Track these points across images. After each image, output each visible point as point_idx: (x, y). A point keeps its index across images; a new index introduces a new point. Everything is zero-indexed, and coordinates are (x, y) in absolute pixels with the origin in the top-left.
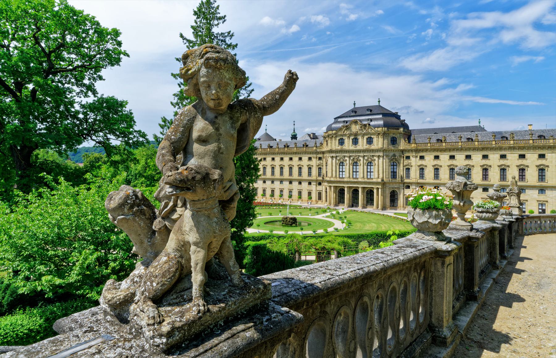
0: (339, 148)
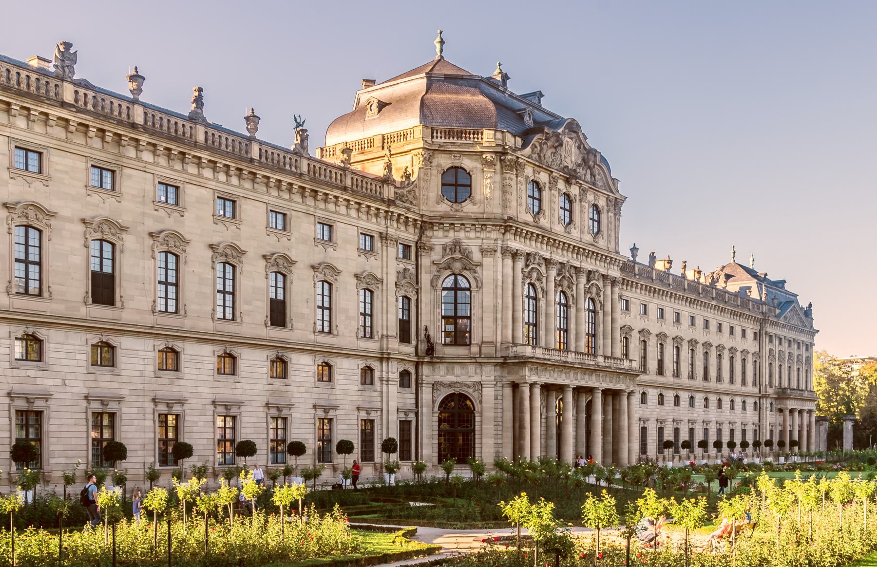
0: (529, 218)
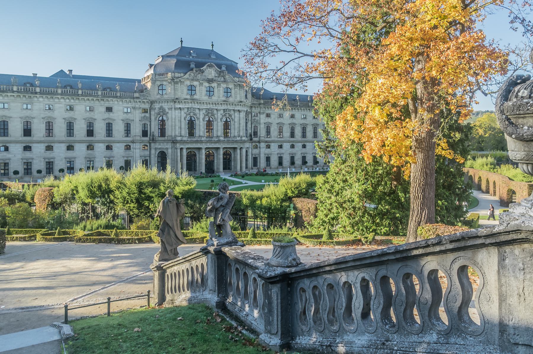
0: (188, 97)
